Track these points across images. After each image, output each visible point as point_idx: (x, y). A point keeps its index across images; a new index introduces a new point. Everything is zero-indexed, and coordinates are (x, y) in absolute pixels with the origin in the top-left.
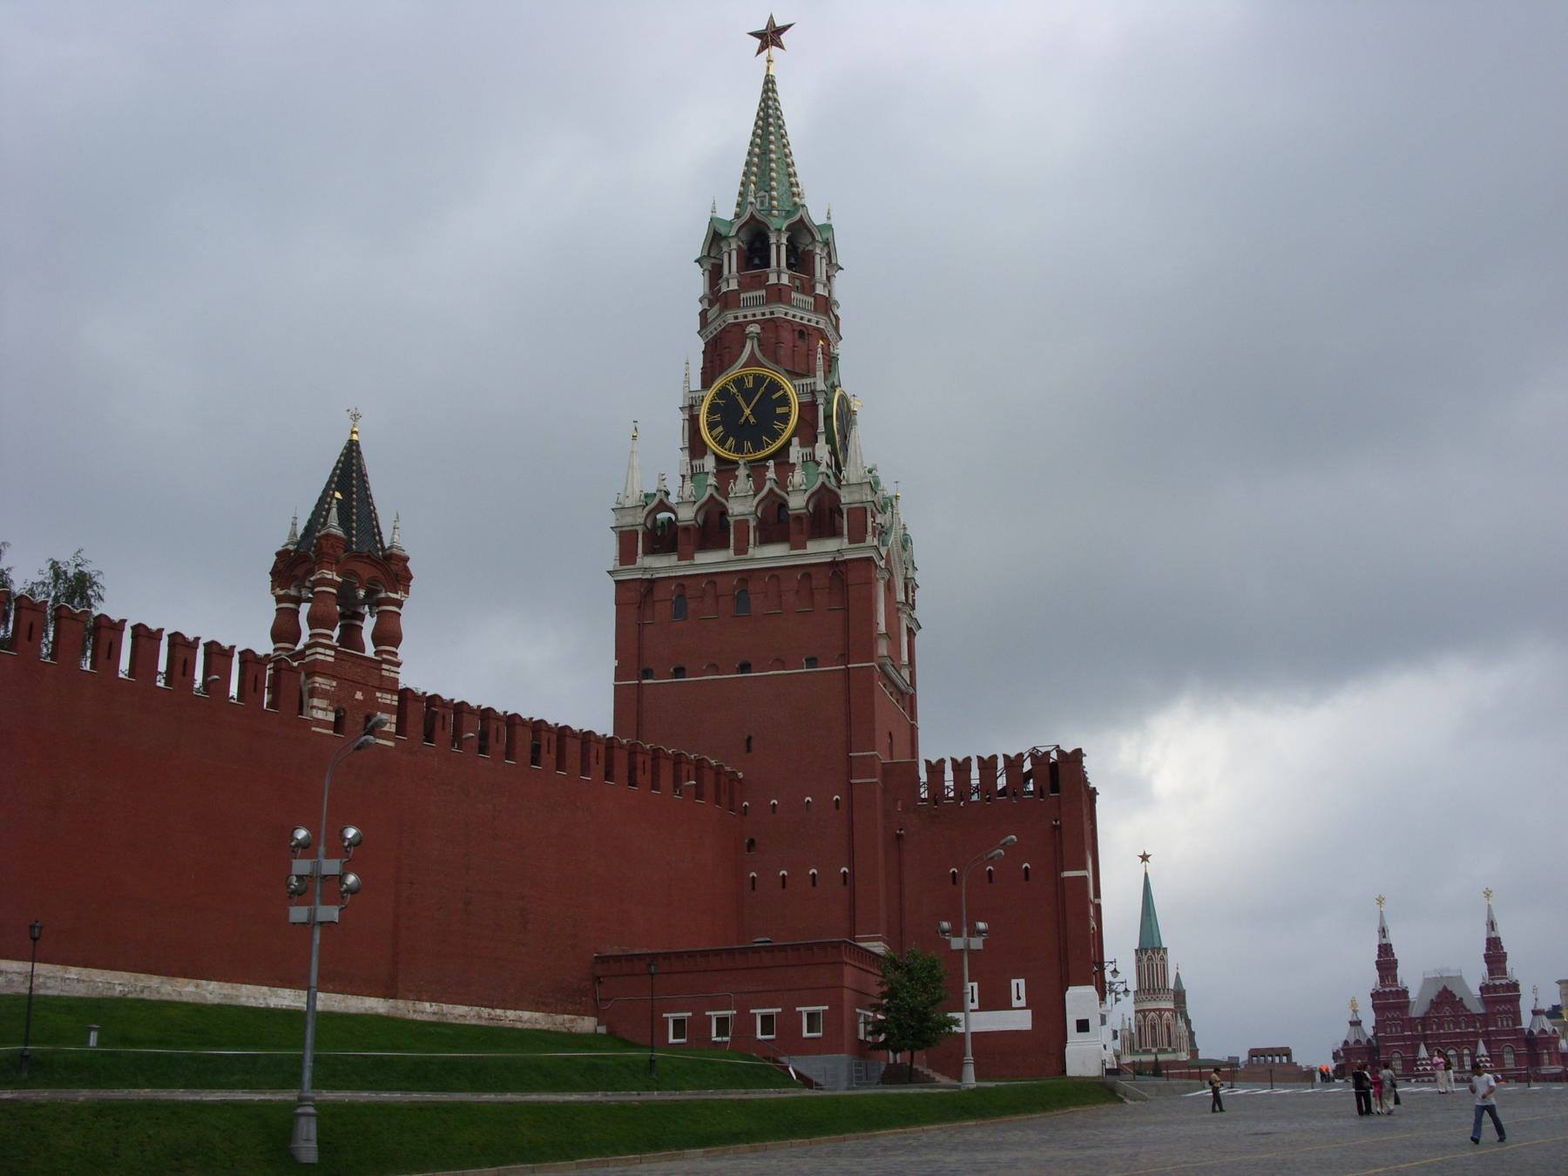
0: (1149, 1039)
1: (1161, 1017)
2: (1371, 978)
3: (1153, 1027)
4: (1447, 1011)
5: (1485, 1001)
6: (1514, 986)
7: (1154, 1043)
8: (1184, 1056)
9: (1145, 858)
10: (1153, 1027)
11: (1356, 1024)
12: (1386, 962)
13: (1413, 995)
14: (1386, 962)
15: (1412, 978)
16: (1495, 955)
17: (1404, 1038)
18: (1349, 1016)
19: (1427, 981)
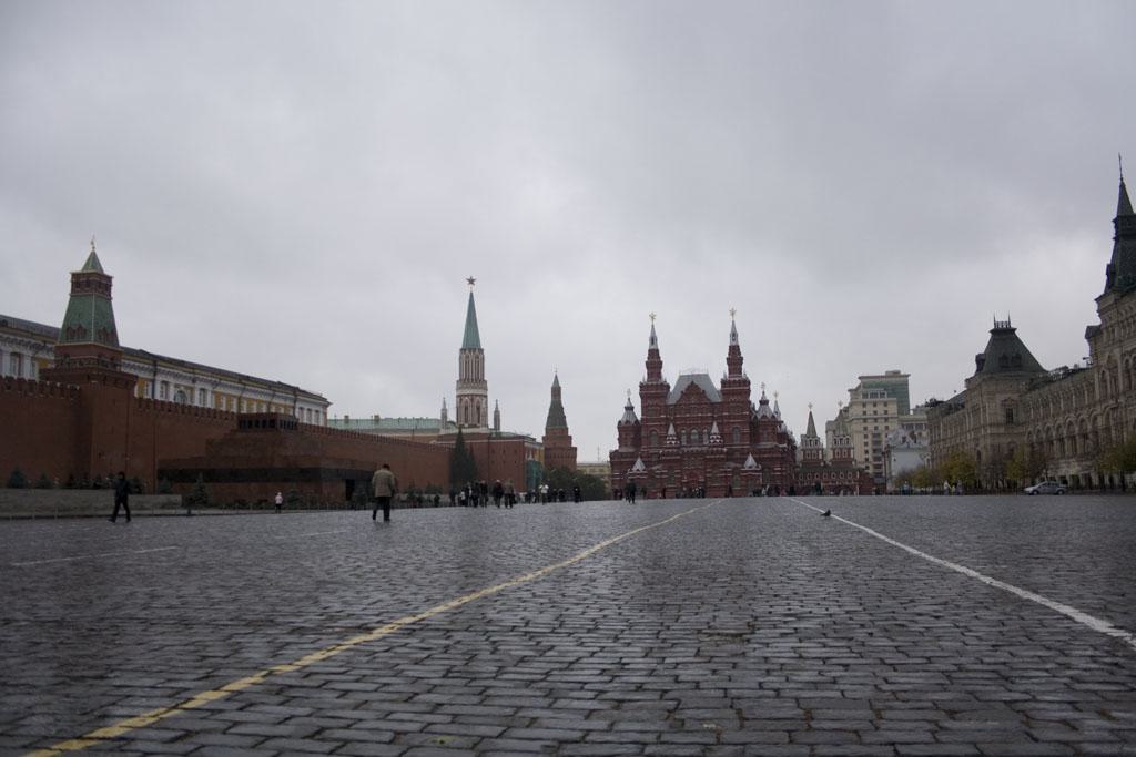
0: (463, 419)
1: (472, 400)
2: (642, 374)
3: (466, 408)
4: (693, 400)
5: (724, 393)
6: (747, 383)
7: (466, 421)
8: (482, 430)
9: (471, 281)
10: (466, 408)
11: (630, 409)
12: (654, 363)
13: (671, 390)
14: (654, 363)
15: (671, 375)
16: (735, 358)
17: (660, 420)
18: (625, 404)
19: (682, 378)
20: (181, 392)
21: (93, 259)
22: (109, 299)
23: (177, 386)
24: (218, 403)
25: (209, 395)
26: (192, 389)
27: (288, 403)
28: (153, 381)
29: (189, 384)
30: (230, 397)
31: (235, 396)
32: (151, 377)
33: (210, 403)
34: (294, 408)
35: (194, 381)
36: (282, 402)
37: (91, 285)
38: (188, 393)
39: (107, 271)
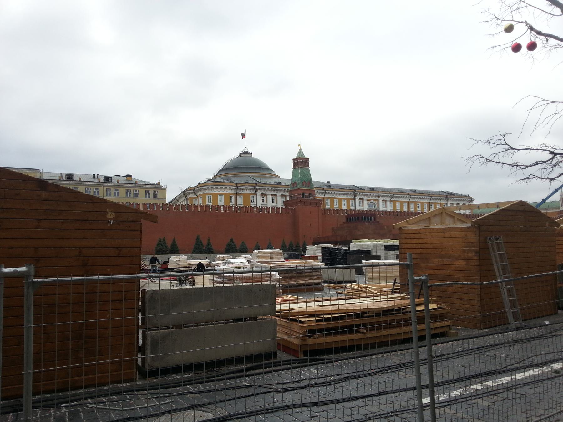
20: (372, 203)
21: (301, 151)
22: (308, 168)
23: (368, 200)
24: (395, 206)
25: (388, 203)
26: (378, 201)
27: (442, 202)
28: (355, 199)
29: (376, 198)
30: (402, 203)
31: (405, 202)
32: (353, 197)
33: (389, 208)
34: (447, 204)
35: (379, 197)
36: (439, 202)
37: (301, 163)
38: (376, 203)
39: (306, 156)
